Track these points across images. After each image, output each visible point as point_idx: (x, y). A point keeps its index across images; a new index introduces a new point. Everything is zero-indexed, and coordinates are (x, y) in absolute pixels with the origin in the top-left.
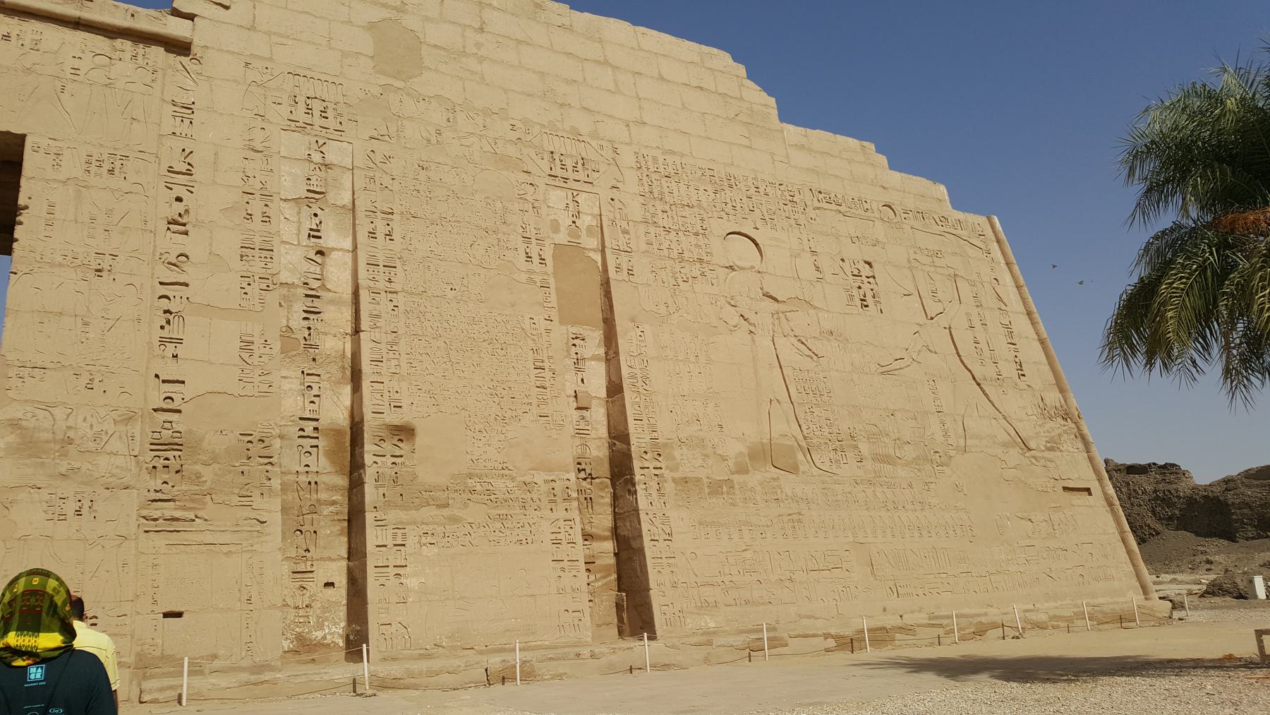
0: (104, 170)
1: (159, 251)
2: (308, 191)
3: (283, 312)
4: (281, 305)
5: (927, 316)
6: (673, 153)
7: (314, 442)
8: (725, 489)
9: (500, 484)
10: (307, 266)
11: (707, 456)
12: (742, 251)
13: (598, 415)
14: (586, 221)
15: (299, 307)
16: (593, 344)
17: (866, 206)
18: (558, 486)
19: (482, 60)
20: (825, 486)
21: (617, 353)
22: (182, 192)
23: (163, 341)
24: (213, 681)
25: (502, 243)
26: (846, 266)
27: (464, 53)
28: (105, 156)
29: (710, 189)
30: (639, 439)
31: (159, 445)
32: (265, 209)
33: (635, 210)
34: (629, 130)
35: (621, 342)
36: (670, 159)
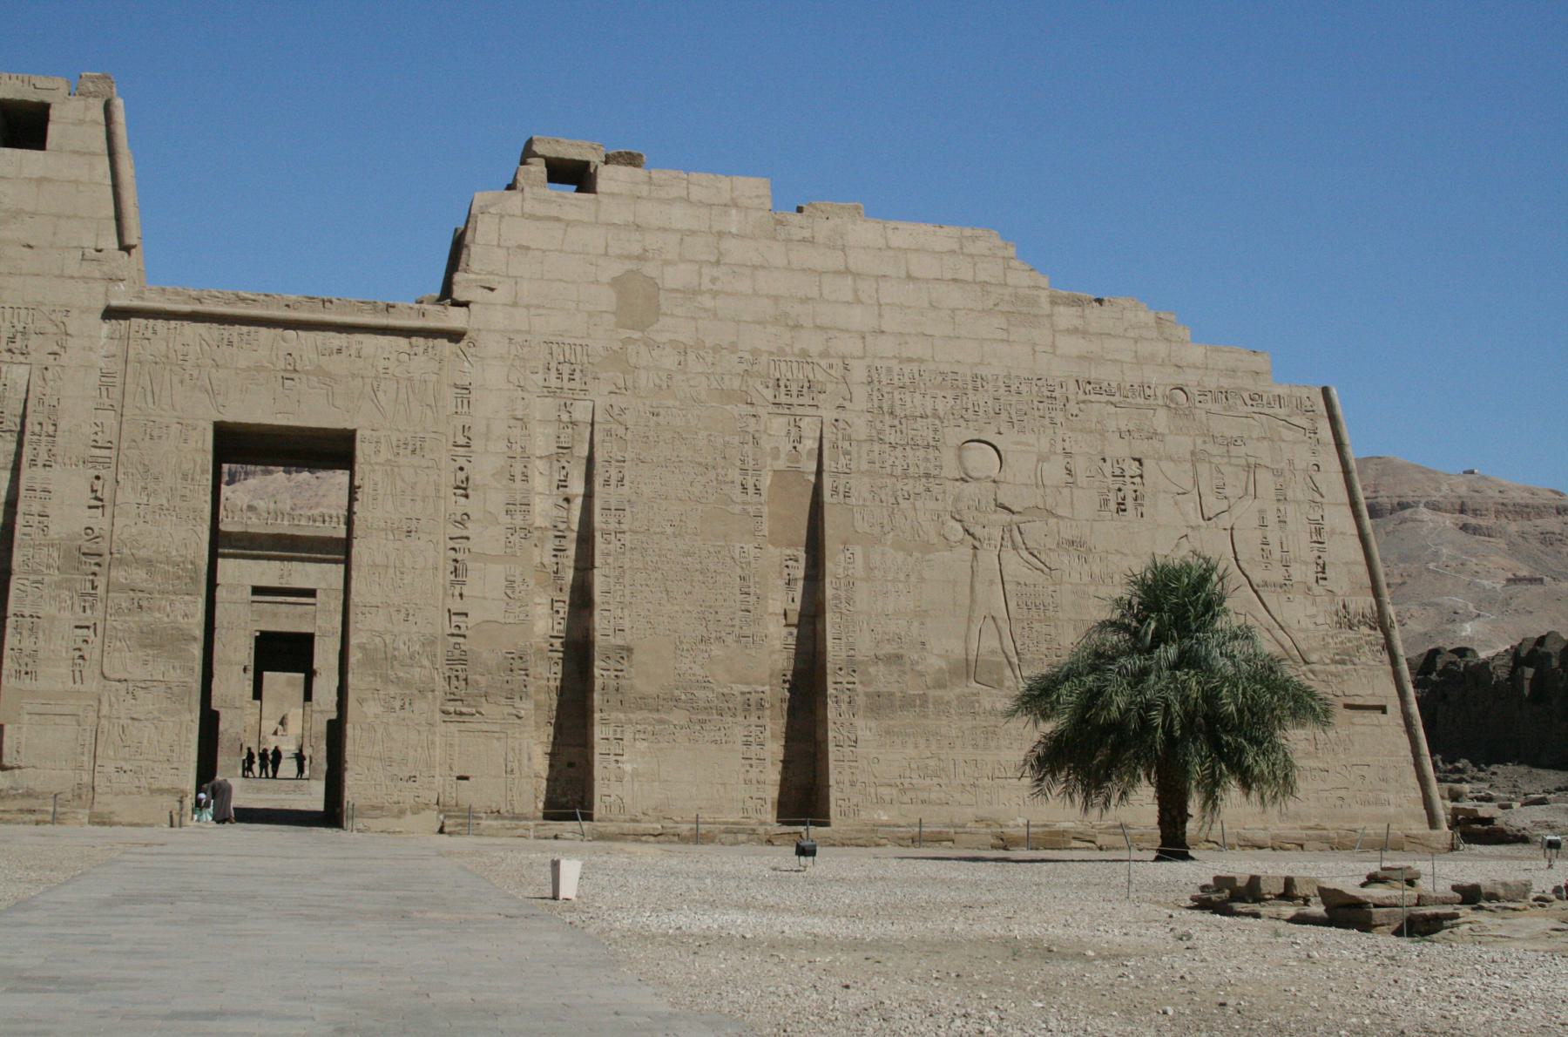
0: (409, 451)
1: (448, 512)
2: (559, 447)
3: (537, 551)
4: (536, 546)
9: (701, 694)
10: (555, 512)
11: (905, 673)
12: (981, 460)
17: (1148, 392)
18: (754, 698)
22: (462, 462)
25: (720, 478)
27: (697, 292)
28: (409, 439)
29: (950, 394)
31: (450, 661)
32: (525, 470)
33: (861, 429)
34: (864, 343)
36: (907, 369)
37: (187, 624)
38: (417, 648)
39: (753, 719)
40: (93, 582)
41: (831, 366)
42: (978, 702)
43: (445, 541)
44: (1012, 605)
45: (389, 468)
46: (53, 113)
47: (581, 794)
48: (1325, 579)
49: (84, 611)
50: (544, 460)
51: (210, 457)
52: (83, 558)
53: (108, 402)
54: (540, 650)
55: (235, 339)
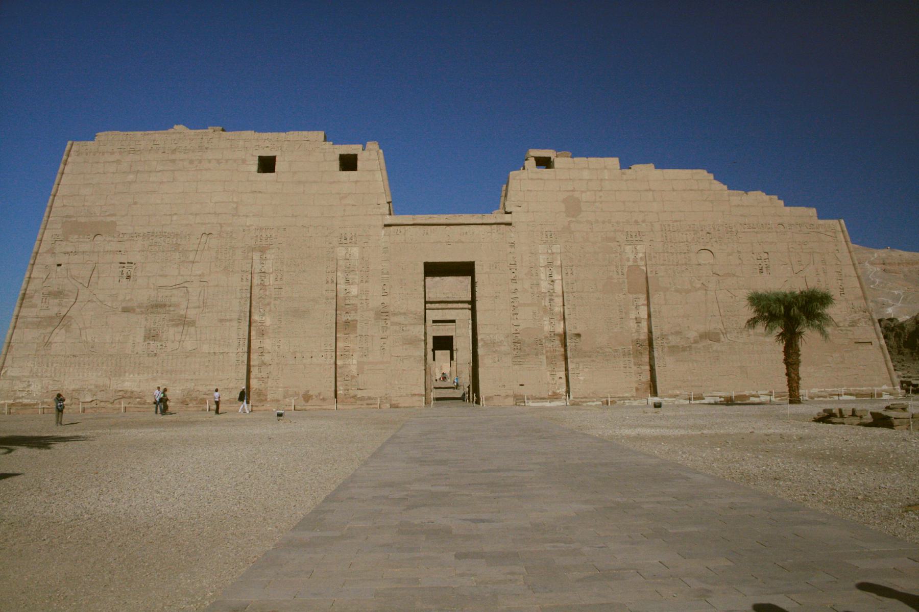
3: (543, 301)
4: (542, 299)
6: (676, 221)
7: (554, 338)
10: (549, 286)
11: (682, 338)
12: (705, 257)
13: (644, 324)
14: (640, 255)
15: (547, 299)
16: (642, 300)
19: (601, 202)
21: (650, 304)
22: (513, 270)
23: (513, 315)
27: (595, 202)
30: (656, 333)
31: (515, 343)
35: (651, 300)
37: (420, 335)
38: (503, 338)
40: (385, 322)
43: (509, 300)
45: (487, 276)
46: (358, 157)
48: (844, 294)
51: (423, 275)
52: (382, 314)
54: (546, 337)
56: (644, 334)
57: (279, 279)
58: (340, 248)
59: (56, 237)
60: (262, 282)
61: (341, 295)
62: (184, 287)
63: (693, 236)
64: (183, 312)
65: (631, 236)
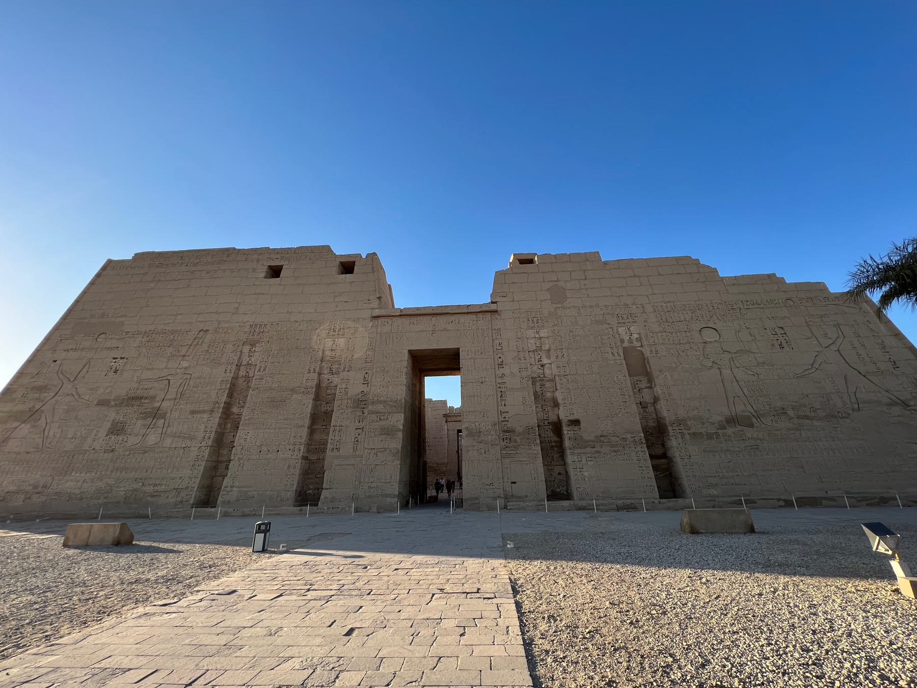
5: (822, 347)
6: (669, 302)
7: (549, 427)
8: (715, 436)
12: (709, 335)
14: (636, 336)
20: (770, 432)
22: (500, 355)
24: (527, 504)
26: (768, 331)
36: (668, 305)
39: (639, 449)
40: (363, 411)
41: (637, 307)
42: (744, 434)
43: (496, 384)
44: (745, 391)
47: (566, 487)
48: (898, 367)
49: (359, 422)
50: (532, 352)
53: (371, 347)
55: (415, 322)
56: (654, 420)
57: (262, 370)
58: (329, 339)
59: (64, 336)
60: (247, 374)
61: (324, 385)
62: (167, 379)
63: (691, 315)
64: (157, 405)
65: (623, 318)
